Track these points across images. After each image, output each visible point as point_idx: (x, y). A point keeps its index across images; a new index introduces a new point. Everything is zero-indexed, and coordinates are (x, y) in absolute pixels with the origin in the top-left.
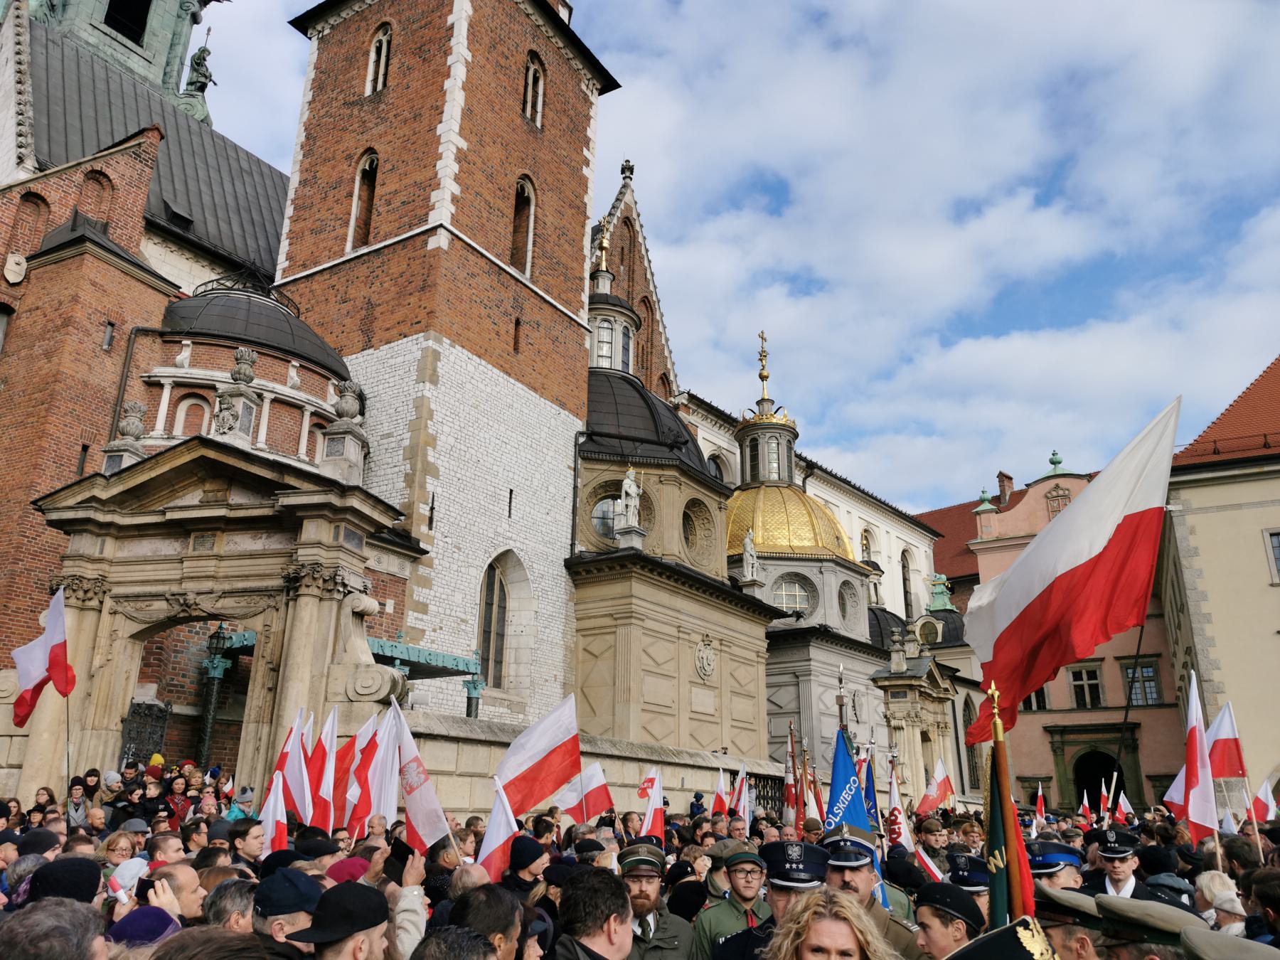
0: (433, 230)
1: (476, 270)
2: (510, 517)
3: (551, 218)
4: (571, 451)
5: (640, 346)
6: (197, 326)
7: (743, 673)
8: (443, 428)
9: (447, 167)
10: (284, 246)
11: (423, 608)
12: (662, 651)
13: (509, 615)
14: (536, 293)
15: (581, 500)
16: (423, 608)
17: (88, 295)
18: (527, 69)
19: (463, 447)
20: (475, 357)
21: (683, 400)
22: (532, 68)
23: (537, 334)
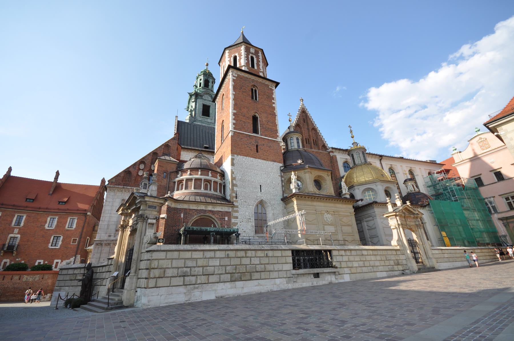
1: (242, 137)
2: (261, 191)
3: (264, 119)
4: (279, 171)
7: (345, 220)
11: (237, 218)
14: (262, 138)
15: (284, 183)
16: (237, 218)
18: (252, 89)
19: (244, 178)
20: (245, 157)
21: (330, 150)
22: (254, 89)
23: (264, 147)
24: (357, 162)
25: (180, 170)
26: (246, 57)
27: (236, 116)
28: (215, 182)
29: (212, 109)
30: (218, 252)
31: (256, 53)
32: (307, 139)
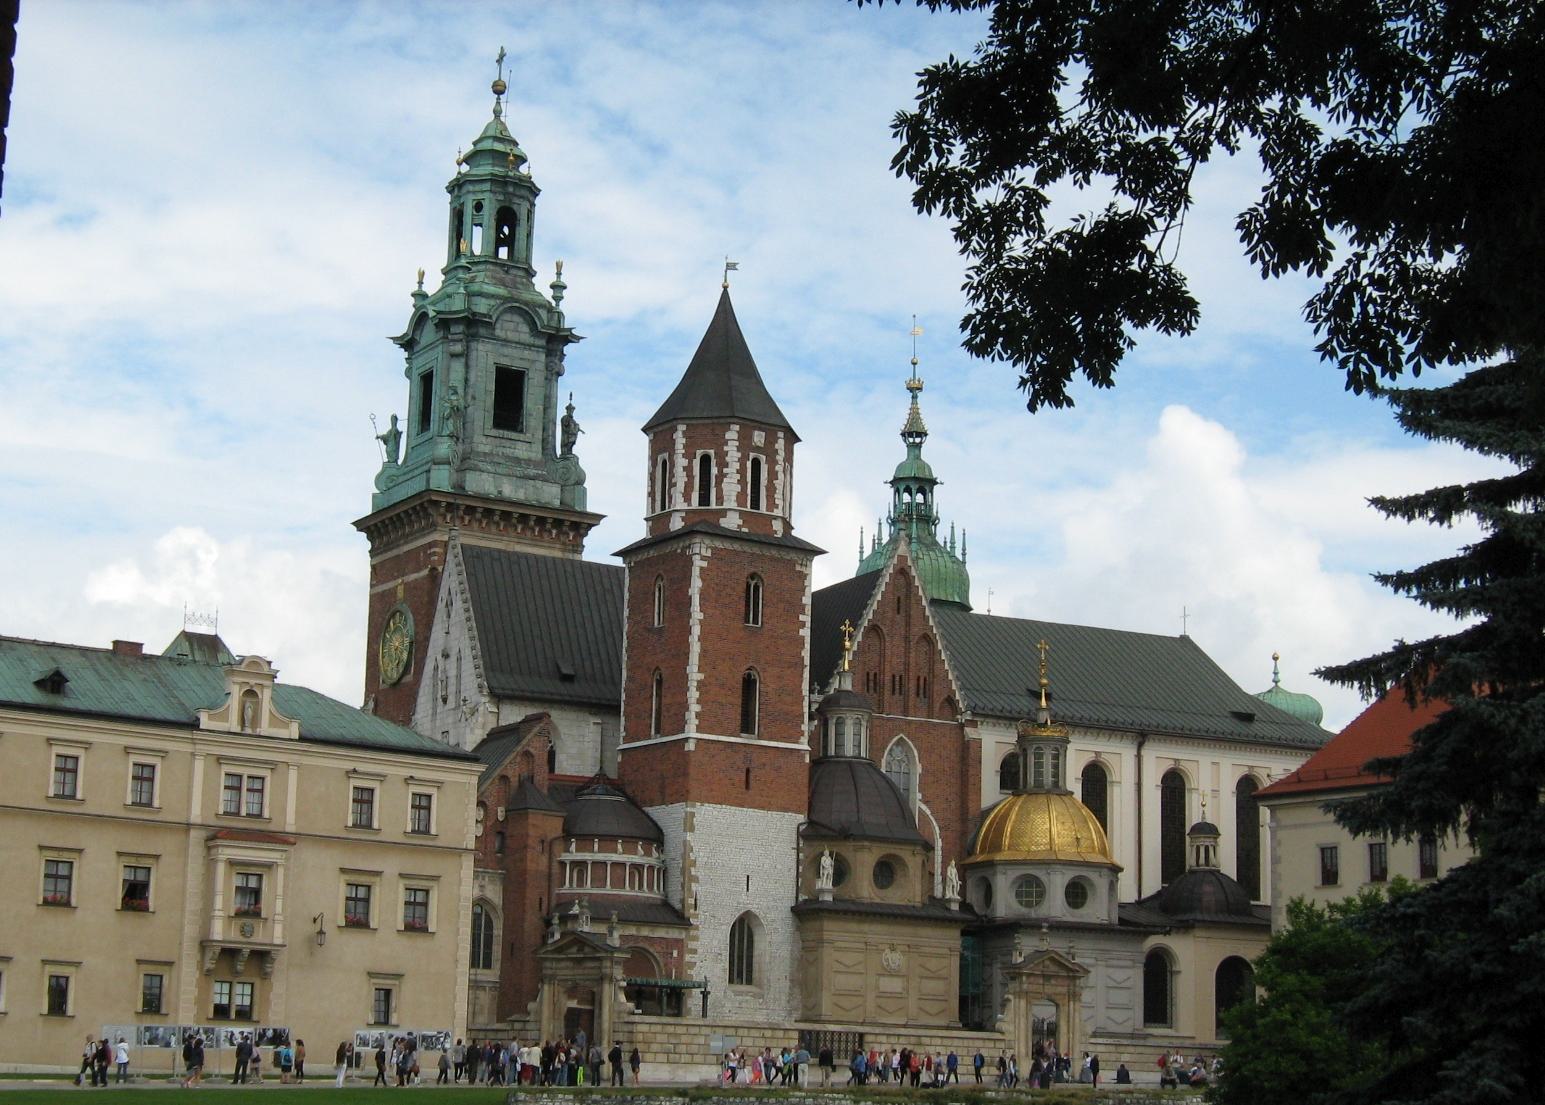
0: (686, 740)
4: (795, 836)
5: (922, 681)
6: (577, 831)
7: (933, 964)
8: (699, 854)
9: (693, 694)
10: (623, 719)
11: (695, 951)
12: (849, 959)
13: (756, 945)
16: (695, 951)
17: (532, 832)
18: (748, 586)
22: (753, 583)
23: (764, 772)
24: (1031, 780)
25: (574, 836)
26: (738, 472)
27: (703, 689)
28: (651, 868)
29: (530, 391)
30: (704, 1028)
31: (771, 441)
32: (897, 678)
